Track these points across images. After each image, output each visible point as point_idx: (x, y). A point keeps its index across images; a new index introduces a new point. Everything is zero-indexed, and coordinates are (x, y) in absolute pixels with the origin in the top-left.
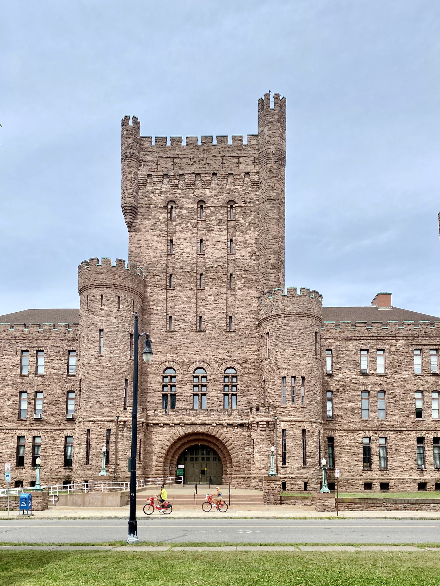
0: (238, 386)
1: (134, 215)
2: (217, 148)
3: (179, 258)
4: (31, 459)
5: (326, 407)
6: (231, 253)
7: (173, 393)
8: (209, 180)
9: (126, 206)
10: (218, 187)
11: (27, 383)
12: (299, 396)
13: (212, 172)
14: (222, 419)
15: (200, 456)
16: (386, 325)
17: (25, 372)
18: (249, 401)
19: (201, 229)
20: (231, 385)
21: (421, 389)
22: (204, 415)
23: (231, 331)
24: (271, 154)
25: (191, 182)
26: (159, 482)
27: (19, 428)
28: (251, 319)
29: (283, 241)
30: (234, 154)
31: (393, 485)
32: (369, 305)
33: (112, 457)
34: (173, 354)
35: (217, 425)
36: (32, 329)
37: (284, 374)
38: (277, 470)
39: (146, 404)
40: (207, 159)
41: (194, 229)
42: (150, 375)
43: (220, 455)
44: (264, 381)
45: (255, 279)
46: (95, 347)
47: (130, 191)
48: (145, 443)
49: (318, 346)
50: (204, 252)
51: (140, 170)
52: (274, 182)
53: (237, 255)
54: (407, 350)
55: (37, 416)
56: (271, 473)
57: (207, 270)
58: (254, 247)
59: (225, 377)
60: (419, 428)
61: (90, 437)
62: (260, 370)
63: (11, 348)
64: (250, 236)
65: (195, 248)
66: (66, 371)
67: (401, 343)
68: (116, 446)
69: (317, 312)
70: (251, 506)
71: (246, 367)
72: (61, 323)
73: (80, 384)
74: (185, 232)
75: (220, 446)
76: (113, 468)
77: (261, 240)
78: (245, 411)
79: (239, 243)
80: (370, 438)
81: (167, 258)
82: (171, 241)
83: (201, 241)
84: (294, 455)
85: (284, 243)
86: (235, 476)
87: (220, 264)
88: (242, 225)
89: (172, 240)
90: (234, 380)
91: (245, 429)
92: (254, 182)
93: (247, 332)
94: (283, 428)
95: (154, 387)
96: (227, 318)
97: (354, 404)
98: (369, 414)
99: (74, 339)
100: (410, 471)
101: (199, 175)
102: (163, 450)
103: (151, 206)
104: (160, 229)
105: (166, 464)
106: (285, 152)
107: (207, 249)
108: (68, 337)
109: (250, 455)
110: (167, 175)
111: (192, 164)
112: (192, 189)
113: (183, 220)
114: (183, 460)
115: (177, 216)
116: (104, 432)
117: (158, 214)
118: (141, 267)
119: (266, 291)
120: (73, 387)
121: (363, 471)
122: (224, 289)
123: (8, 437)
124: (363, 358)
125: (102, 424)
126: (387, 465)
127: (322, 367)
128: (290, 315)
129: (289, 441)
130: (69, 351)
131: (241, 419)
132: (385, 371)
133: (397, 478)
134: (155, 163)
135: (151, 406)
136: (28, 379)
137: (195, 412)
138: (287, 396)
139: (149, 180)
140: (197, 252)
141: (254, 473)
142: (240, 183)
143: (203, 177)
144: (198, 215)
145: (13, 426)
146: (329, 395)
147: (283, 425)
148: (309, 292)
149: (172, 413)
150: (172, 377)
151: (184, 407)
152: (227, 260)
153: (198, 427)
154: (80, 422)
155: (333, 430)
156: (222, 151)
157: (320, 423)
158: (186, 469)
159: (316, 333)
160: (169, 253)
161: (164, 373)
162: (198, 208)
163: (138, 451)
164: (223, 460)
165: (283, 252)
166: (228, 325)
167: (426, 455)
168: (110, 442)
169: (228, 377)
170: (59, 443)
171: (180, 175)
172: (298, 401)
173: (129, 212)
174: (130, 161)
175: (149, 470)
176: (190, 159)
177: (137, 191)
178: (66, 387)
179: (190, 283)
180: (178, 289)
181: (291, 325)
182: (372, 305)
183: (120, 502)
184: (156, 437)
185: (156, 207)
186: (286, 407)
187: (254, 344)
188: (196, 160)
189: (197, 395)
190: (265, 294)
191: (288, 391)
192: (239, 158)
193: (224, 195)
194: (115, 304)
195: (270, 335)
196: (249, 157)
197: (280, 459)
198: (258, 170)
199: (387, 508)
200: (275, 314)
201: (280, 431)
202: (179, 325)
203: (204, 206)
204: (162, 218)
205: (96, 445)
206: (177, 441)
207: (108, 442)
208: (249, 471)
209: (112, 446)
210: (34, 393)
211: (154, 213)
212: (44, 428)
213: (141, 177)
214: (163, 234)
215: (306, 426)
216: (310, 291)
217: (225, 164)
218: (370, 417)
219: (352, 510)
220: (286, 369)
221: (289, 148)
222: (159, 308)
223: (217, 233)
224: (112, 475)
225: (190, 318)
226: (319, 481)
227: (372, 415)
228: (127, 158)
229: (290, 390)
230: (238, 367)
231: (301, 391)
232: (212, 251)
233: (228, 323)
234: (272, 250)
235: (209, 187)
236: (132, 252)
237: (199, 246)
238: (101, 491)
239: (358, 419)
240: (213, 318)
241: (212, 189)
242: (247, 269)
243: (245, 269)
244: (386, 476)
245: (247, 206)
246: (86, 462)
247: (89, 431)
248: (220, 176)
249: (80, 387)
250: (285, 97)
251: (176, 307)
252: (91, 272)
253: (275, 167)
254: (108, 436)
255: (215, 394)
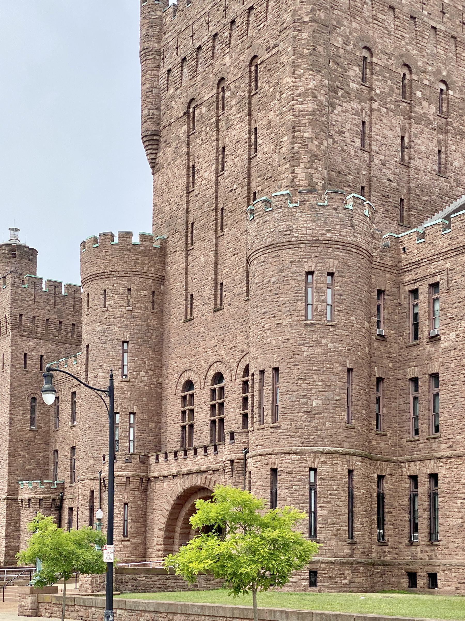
65: (214, 167)
117: (179, 130)
162: (218, 93)
193: (246, 51)
202: (197, 306)
223: (238, 126)
242: (269, 175)
243: (268, 176)
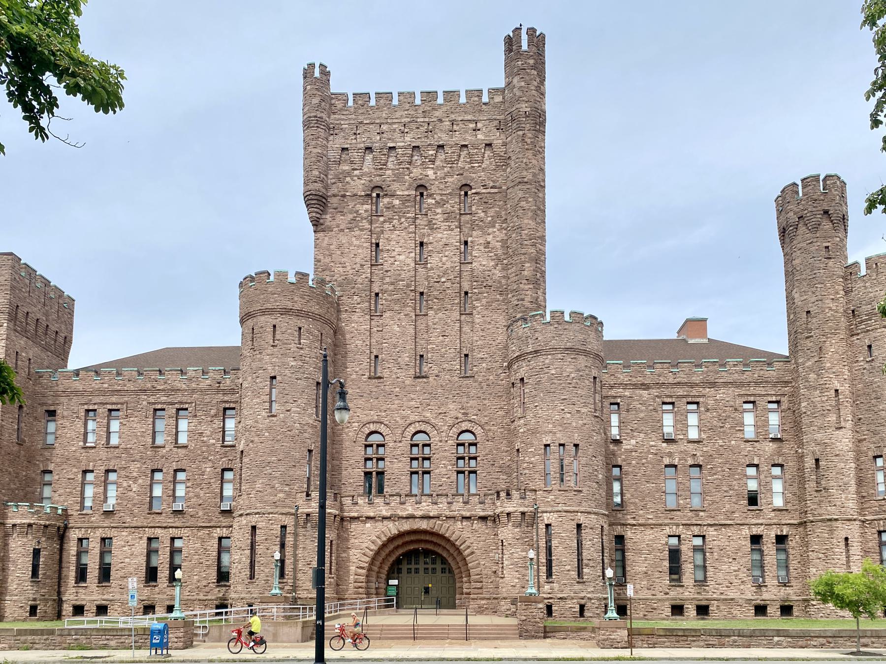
0: (478, 459)
1: (322, 208)
2: (444, 109)
3: (389, 269)
4: (168, 572)
5: (612, 490)
6: (466, 262)
7: (380, 470)
8: (432, 155)
9: (310, 195)
10: (445, 165)
11: (162, 457)
12: (571, 474)
13: (436, 143)
14: (454, 510)
15: (421, 566)
16: (700, 366)
17: (160, 441)
18: (495, 481)
19: (421, 227)
20: (467, 458)
21: (755, 462)
22: (428, 504)
23: (467, 377)
24: (524, 116)
25: (406, 158)
26: (360, 605)
27: (150, 525)
28: (497, 358)
29: (544, 243)
30: (469, 117)
31: (715, 609)
32: (674, 336)
33: (288, 568)
34: (380, 411)
35: (447, 518)
36: (169, 376)
37: (547, 439)
38: (539, 587)
39: (340, 488)
40: (429, 124)
41: (411, 226)
42: (347, 444)
43: (452, 565)
44: (518, 450)
45: (501, 298)
46: (264, 402)
47: (316, 173)
48: (338, 547)
49: (598, 397)
50: (426, 260)
51: (331, 143)
52: (530, 157)
53: (474, 264)
54: (732, 403)
55: (178, 506)
56: (530, 591)
57: (431, 287)
58: (500, 252)
59: (458, 445)
60: (753, 520)
61: (255, 537)
62: (512, 433)
63: (139, 406)
64: (493, 237)
65: (413, 255)
66: (221, 439)
67: (724, 393)
68: (295, 551)
69: (596, 347)
70: (499, 641)
71: (490, 430)
72: (214, 368)
73: (241, 458)
74: (398, 232)
75: (452, 551)
76: (291, 584)
77: (511, 241)
78: (490, 497)
79: (478, 247)
80: (679, 536)
81: (371, 269)
82: (377, 245)
83: (422, 244)
84: (564, 563)
85: (544, 245)
86: (476, 596)
87: (450, 278)
88: (482, 221)
89: (379, 243)
90: (473, 449)
91: (490, 524)
92: (499, 158)
93: (491, 377)
94: (546, 523)
95: (352, 461)
96: (461, 357)
97: (654, 485)
98: (677, 501)
99: (232, 391)
100: (742, 587)
101: (417, 149)
102: (365, 557)
103: (348, 194)
104: (361, 228)
105: (371, 578)
106: (545, 113)
107: (430, 256)
108: (224, 388)
109: (498, 563)
110: (371, 148)
111: (407, 133)
112: (408, 168)
113: (395, 214)
114: (396, 573)
115: (386, 208)
116: (277, 530)
118: (332, 283)
119: (519, 316)
120: (230, 462)
121: (669, 588)
122: (456, 315)
123: (132, 539)
124: (665, 416)
125: (273, 518)
126: (705, 577)
127: (604, 428)
128: (554, 352)
129: (556, 542)
130: (225, 409)
131: (483, 509)
132: (700, 435)
133: (722, 597)
134: (353, 132)
135: (347, 490)
136: (165, 451)
137: (413, 499)
138: (552, 473)
139: (343, 156)
140: (415, 261)
141: (504, 592)
142: (478, 159)
143: (424, 151)
144: (417, 206)
145: (142, 522)
146: (616, 471)
147: (547, 518)
148: (583, 318)
149: (379, 500)
150: (378, 446)
151: (398, 491)
152: (460, 271)
153: (418, 521)
154: (241, 515)
155: (624, 525)
156: (452, 112)
157: (602, 514)
158: (400, 586)
159: (595, 378)
160: (373, 262)
161: (366, 440)
163: (327, 559)
164: (456, 571)
165: (544, 259)
166: (463, 368)
167: (765, 562)
168: (286, 546)
169: (463, 445)
170: (209, 548)
171: (390, 148)
172: (569, 481)
173: (315, 204)
174: (316, 128)
175: (344, 587)
176: (405, 125)
177: (325, 173)
178: (221, 463)
179: (405, 305)
180: (387, 314)
181: (557, 366)
182: (678, 337)
183: (300, 636)
184: (355, 537)
185: (355, 195)
186: (551, 491)
187: (502, 396)
188: (414, 127)
189: (417, 473)
190: (517, 321)
191: (553, 467)
192: (476, 123)
193: (455, 176)
194: (293, 338)
195: (525, 381)
196: (490, 120)
197: (544, 569)
198: (505, 140)
199: (706, 642)
200: (533, 350)
201: (542, 526)
203: (425, 193)
204: (363, 212)
205: (265, 550)
206: (387, 544)
207: (283, 546)
208: (496, 588)
209: (289, 550)
210: (173, 473)
211: (351, 204)
212: (187, 525)
213: (332, 151)
214: (365, 235)
215: (582, 519)
216: (585, 316)
217: (455, 131)
218: (678, 505)
219: (653, 646)
220: (551, 432)
221: (550, 106)
222: (359, 343)
223: (445, 232)
224: (288, 595)
225: (405, 358)
226: (602, 603)
227: (681, 502)
228: (312, 125)
229: (557, 465)
230: (478, 431)
231: (574, 466)
232: (437, 259)
233: (463, 365)
234: (526, 256)
235: (432, 166)
236: (319, 261)
237: (419, 251)
238: (273, 619)
239: (660, 507)
240: (440, 358)
241: (438, 168)
242: (490, 284)
244: (705, 595)
245: (489, 193)
246: (251, 575)
247: (254, 528)
248: (448, 149)
249: (241, 463)
250: (544, 32)
251: (384, 341)
252: (258, 292)
253: (530, 135)
254: (283, 536)
255: (444, 471)
